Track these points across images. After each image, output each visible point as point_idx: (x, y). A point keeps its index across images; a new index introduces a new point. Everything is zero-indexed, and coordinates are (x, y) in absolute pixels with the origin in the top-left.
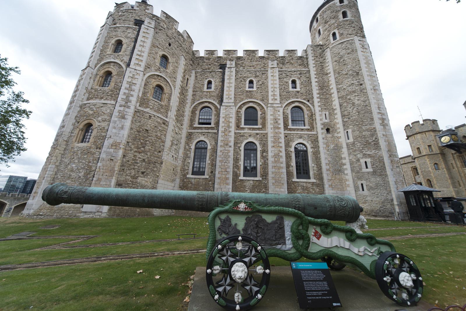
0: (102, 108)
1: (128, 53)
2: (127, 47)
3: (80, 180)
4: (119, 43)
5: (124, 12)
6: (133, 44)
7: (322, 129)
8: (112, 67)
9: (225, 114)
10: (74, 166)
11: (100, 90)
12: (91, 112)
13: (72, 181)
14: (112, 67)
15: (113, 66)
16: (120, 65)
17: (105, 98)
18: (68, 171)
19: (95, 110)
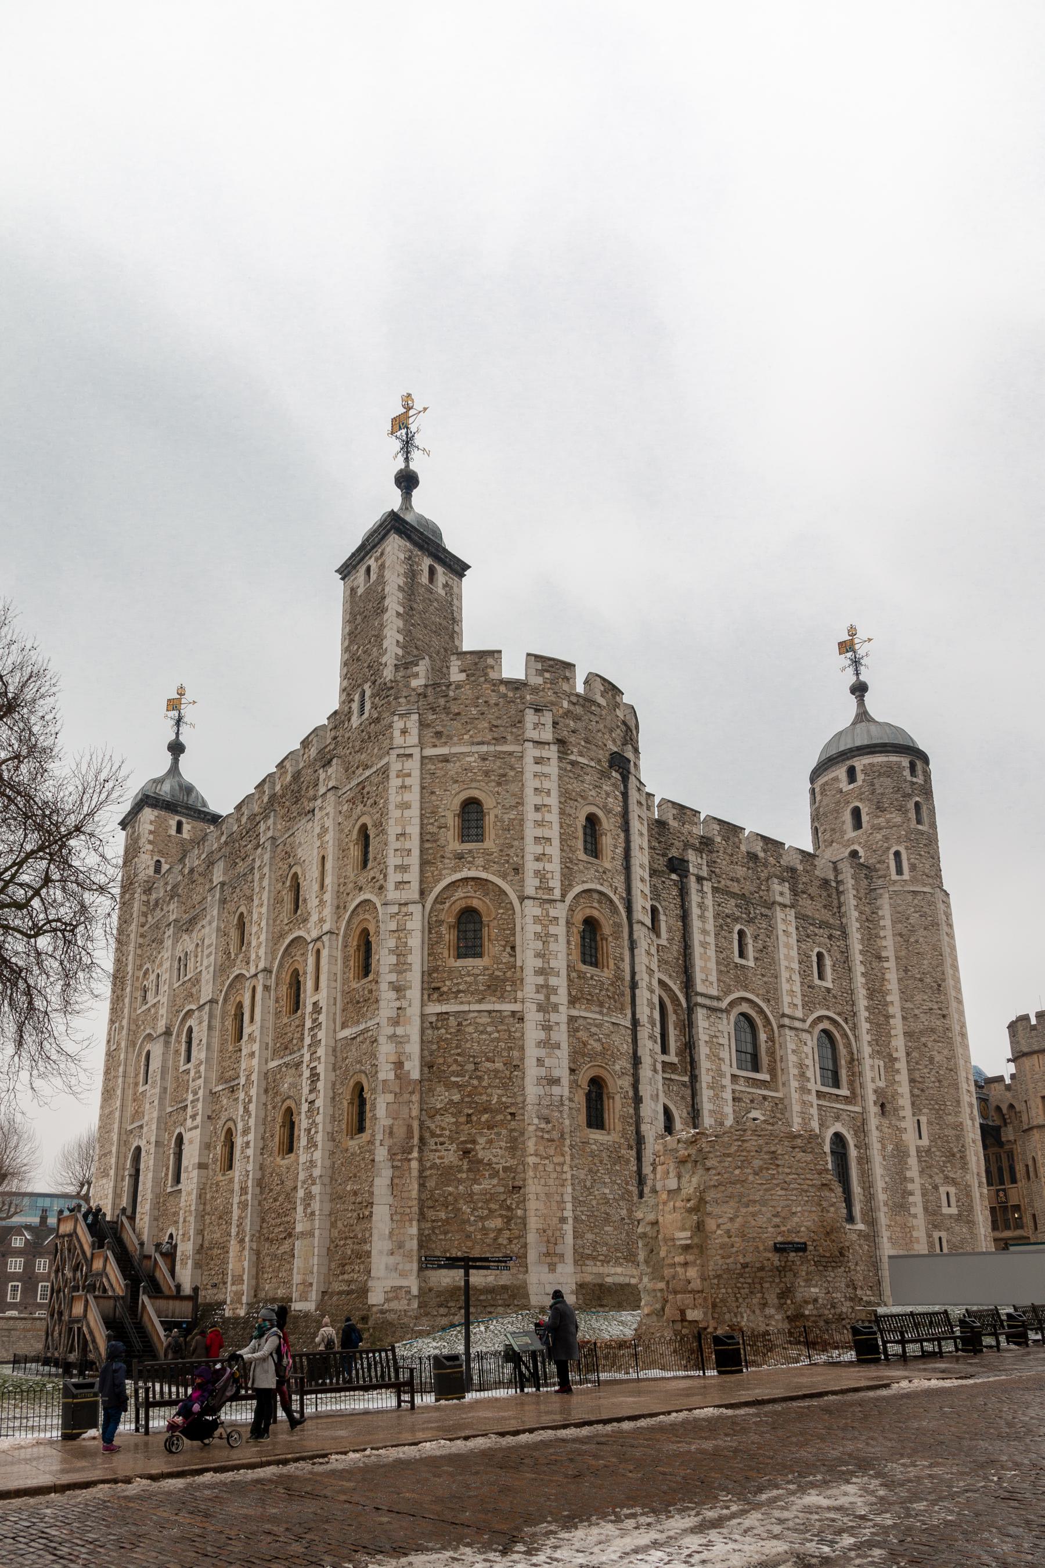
0: (614, 1037)
1: (619, 863)
2: (616, 847)
3: (626, 1227)
4: (592, 821)
5: (574, 704)
6: (622, 835)
7: (875, 1103)
8: (596, 905)
9: (709, 1032)
10: (607, 1191)
11: (592, 978)
12: (598, 1047)
13: (615, 1229)
14: (596, 905)
15: (600, 902)
16: (611, 901)
17: (607, 1005)
18: (598, 1204)
19: (604, 1041)
